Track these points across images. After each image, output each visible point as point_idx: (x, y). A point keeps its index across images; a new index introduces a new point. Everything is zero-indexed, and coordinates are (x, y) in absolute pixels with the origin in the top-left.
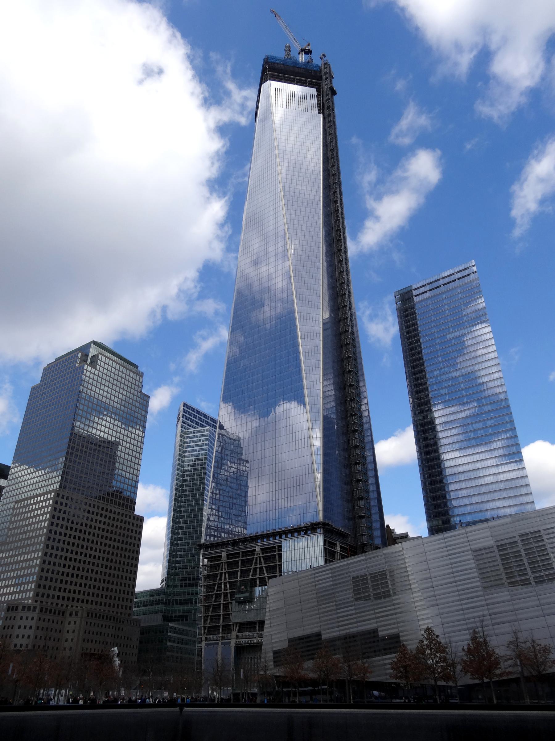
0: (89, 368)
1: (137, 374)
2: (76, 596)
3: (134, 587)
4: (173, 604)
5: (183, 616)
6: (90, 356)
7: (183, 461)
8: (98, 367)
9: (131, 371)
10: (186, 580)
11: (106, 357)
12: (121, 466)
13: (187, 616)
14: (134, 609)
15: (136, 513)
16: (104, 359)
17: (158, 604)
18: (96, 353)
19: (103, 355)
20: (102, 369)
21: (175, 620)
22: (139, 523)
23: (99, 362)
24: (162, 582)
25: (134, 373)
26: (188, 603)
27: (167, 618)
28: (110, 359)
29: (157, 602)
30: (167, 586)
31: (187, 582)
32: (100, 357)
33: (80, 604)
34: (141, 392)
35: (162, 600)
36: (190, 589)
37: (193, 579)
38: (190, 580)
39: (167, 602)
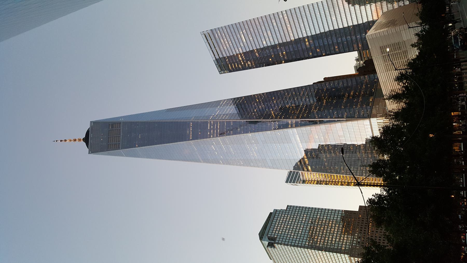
0: (277, 241)
1: (276, 213)
6: (270, 241)
9: (274, 217)
11: (269, 232)
15: (358, 210)
16: (269, 233)
19: (268, 234)
23: (272, 236)
25: (275, 215)
28: (269, 230)
32: (269, 235)
34: (286, 210)
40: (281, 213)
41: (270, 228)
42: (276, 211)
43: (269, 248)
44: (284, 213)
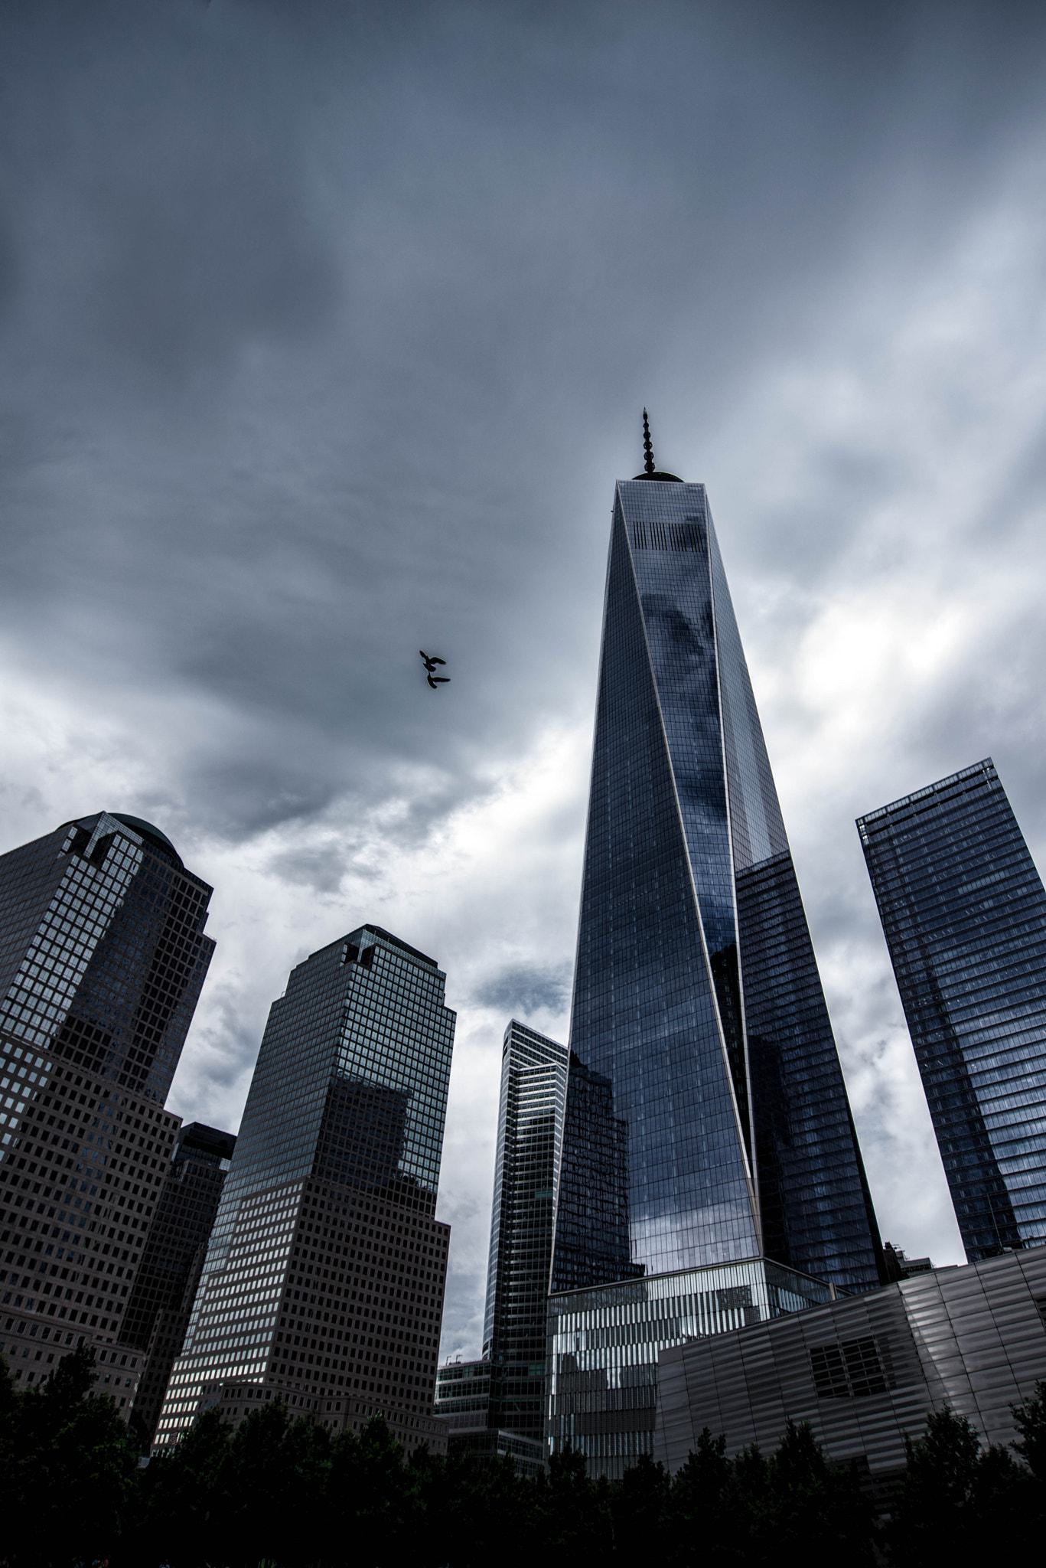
0: (360, 969)
1: (436, 976)
2: (338, 1372)
3: (435, 1357)
5: (523, 1417)
7: (516, 1125)
8: (374, 967)
9: (425, 971)
10: (526, 1346)
11: (387, 950)
12: (411, 1134)
14: (437, 1400)
15: (437, 1218)
16: (383, 952)
18: (371, 944)
19: (381, 947)
20: (379, 970)
21: (509, 1426)
22: (442, 1237)
23: (375, 959)
24: (485, 1349)
25: (430, 974)
27: (496, 1420)
28: (392, 953)
29: (476, 1387)
30: (494, 1356)
32: (377, 950)
33: (343, 1388)
34: (442, 1007)
35: (486, 1383)
37: (539, 1345)
38: (533, 1346)
40: (436, 991)
41: (398, 956)
42: (442, 978)
43: (345, 949)
44: (435, 999)
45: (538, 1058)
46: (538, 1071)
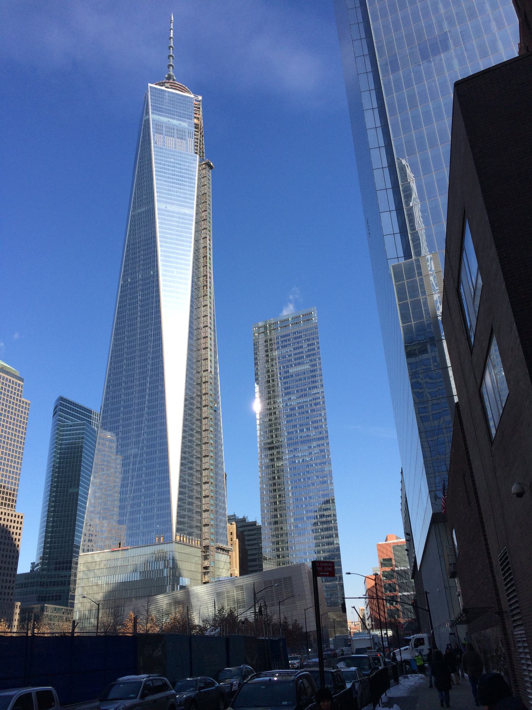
4: (47, 586)
5: (56, 596)
10: (60, 564)
13: (60, 596)
17: (33, 586)
26: (61, 584)
31: (61, 565)
35: (37, 582)
36: (62, 573)
39: (42, 585)
45: (77, 417)
46: (77, 425)
